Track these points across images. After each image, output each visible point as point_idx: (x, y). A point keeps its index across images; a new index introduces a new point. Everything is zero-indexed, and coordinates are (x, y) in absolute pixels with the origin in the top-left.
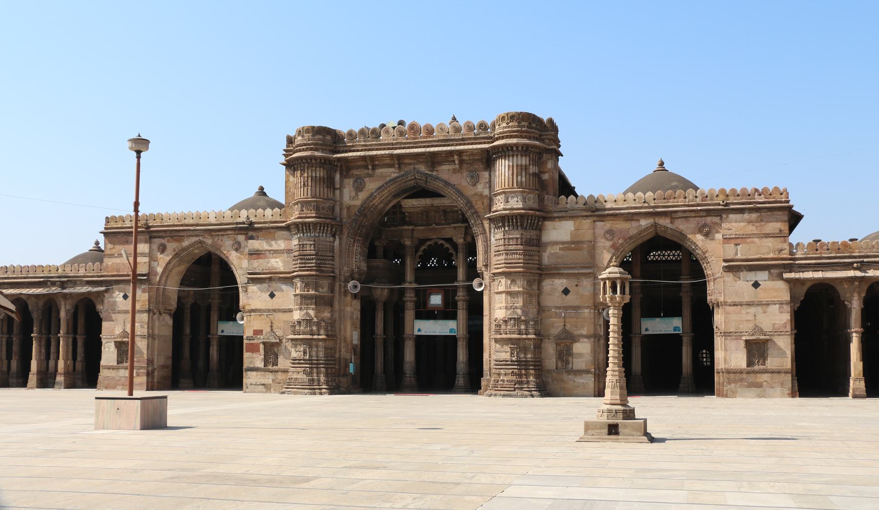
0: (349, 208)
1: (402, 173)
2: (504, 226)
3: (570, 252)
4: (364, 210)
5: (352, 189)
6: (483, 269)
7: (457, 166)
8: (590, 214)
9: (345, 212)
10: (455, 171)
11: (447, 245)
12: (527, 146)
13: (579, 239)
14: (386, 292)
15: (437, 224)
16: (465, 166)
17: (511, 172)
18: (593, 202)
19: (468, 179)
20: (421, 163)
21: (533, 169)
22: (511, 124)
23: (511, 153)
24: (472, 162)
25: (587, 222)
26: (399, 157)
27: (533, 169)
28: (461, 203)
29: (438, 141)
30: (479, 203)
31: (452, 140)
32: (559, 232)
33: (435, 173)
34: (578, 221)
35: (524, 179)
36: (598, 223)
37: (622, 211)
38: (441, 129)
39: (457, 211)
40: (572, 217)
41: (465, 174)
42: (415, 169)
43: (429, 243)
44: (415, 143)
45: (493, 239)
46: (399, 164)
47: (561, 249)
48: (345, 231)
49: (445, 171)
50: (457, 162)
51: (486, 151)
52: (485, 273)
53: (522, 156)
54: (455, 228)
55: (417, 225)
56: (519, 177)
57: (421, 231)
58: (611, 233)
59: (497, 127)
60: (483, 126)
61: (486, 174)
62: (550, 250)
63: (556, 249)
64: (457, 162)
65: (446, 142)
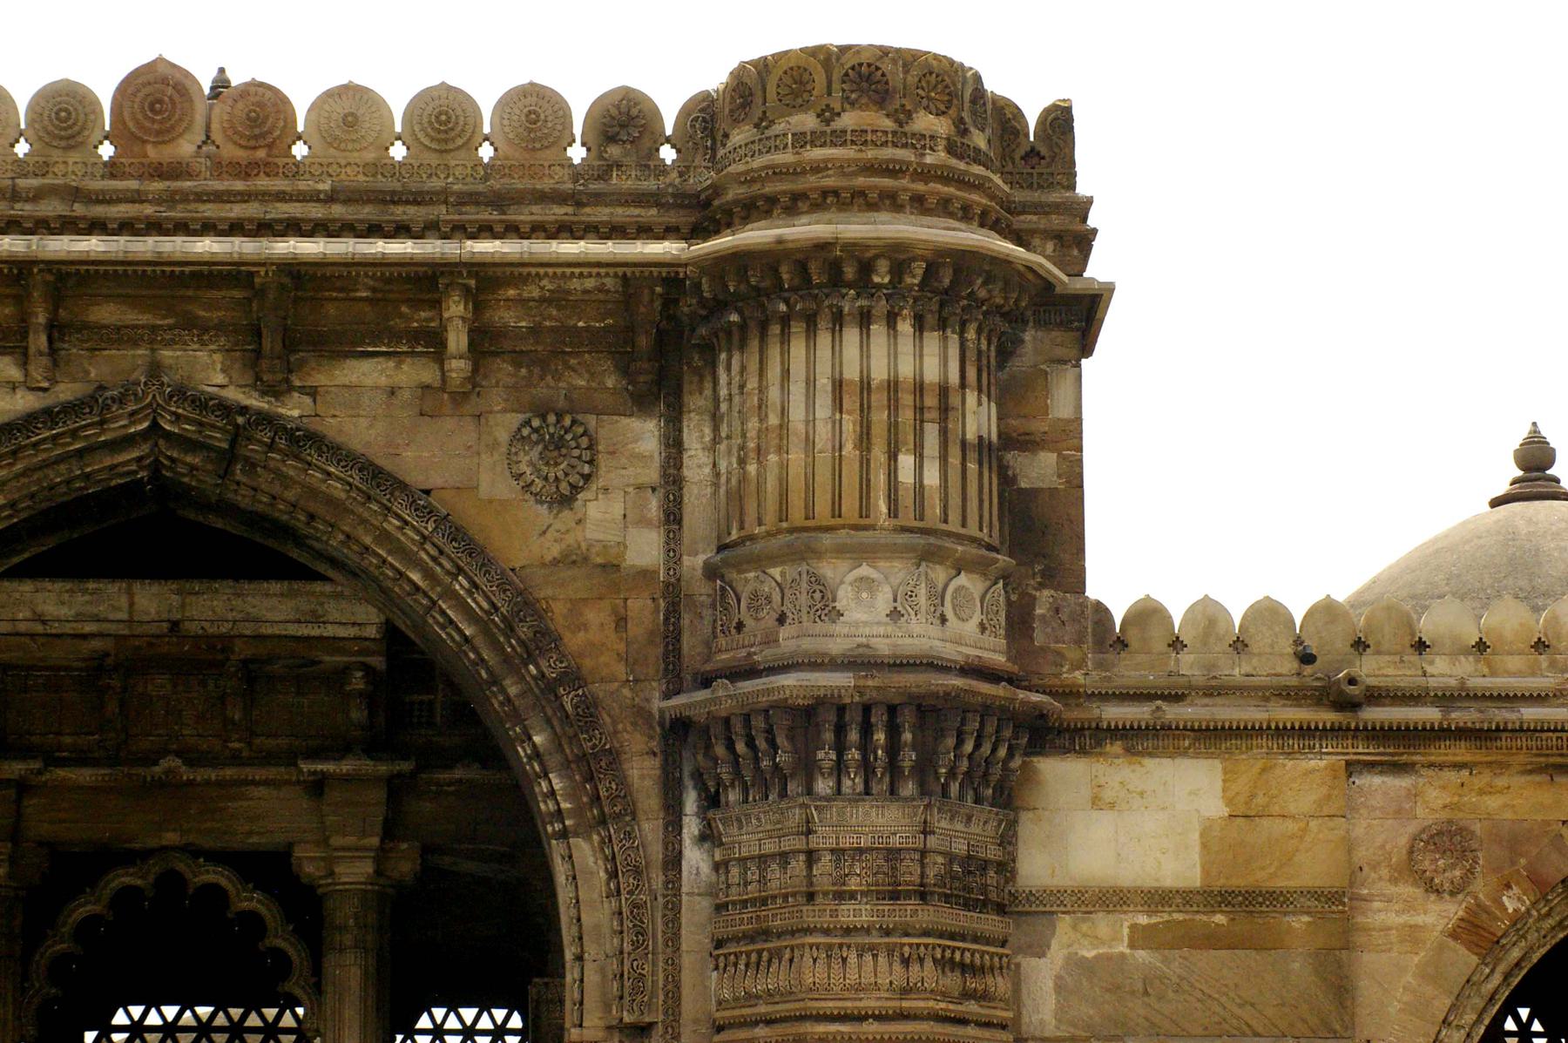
1: (66, 391)
2: (808, 769)
3: (1206, 960)
7: (458, 367)
8: (1328, 717)
10: (434, 401)
11: (250, 900)
12: (964, 262)
13: (1261, 876)
15: (193, 758)
16: (503, 370)
17: (850, 424)
18: (1342, 645)
19: (527, 459)
20: (201, 331)
21: (979, 418)
22: (848, 120)
23: (850, 303)
24: (549, 349)
25: (1305, 777)
26: (71, 280)
27: (979, 418)
28: (457, 620)
29: (331, 198)
30: (597, 617)
31: (418, 199)
32: (1123, 829)
33: (293, 409)
34: (1251, 761)
35: (932, 477)
36: (1374, 781)
37: (1530, 713)
38: (350, 121)
39: (344, 672)
40: (1211, 738)
41: (505, 424)
42: (155, 370)
43: (124, 878)
44: (171, 199)
45: (695, 859)
46: (56, 330)
47: (1140, 937)
49: (361, 399)
50: (457, 340)
51: (671, 278)
53: (920, 325)
54: (318, 786)
55: (52, 761)
56: (906, 461)
58: (1449, 839)
59: (740, 136)
60: (624, 119)
61: (645, 434)
62: (1069, 942)
63: (1109, 937)
64: (457, 340)
65: (384, 203)
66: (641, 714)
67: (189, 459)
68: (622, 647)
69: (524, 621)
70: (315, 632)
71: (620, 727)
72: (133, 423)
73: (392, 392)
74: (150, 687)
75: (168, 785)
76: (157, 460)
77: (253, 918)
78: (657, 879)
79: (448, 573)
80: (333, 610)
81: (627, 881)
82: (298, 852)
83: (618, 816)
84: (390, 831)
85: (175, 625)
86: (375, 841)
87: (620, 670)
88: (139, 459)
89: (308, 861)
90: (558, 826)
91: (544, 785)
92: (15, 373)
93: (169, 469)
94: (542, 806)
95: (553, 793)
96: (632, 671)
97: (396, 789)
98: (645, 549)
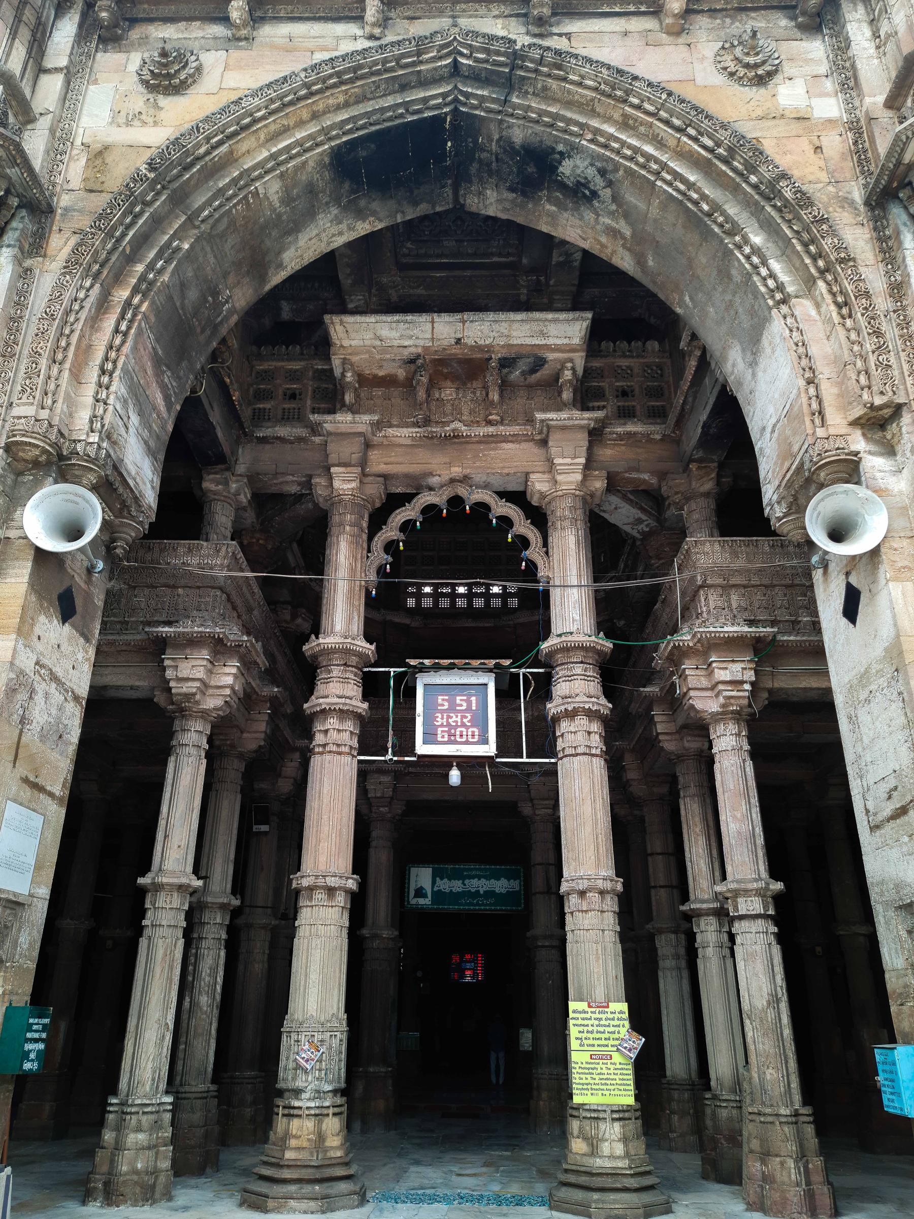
0: (99, 155)
4: (174, 175)
5: (131, 82)
6: (858, 443)
9: (75, 171)
14: (228, 676)
48: (61, 245)
52: (874, 464)
57: (401, 450)
66: (846, 202)
67: (479, 92)
68: (822, 163)
69: (735, 159)
70: (543, 342)
71: (831, 209)
72: (441, 58)
73: (626, 34)
74: (443, 395)
75: (455, 437)
76: (456, 100)
77: (506, 522)
78: (882, 303)
79: (678, 130)
80: (553, 329)
81: (858, 306)
82: (533, 477)
83: (842, 261)
84: (588, 466)
85: (459, 339)
86: (582, 460)
87: (824, 176)
88: (444, 95)
89: (539, 485)
90: (778, 296)
91: (764, 272)
92: (359, 32)
93: (465, 104)
94: (763, 289)
95: (772, 275)
96: (833, 177)
97: (596, 435)
98: (829, 107)
